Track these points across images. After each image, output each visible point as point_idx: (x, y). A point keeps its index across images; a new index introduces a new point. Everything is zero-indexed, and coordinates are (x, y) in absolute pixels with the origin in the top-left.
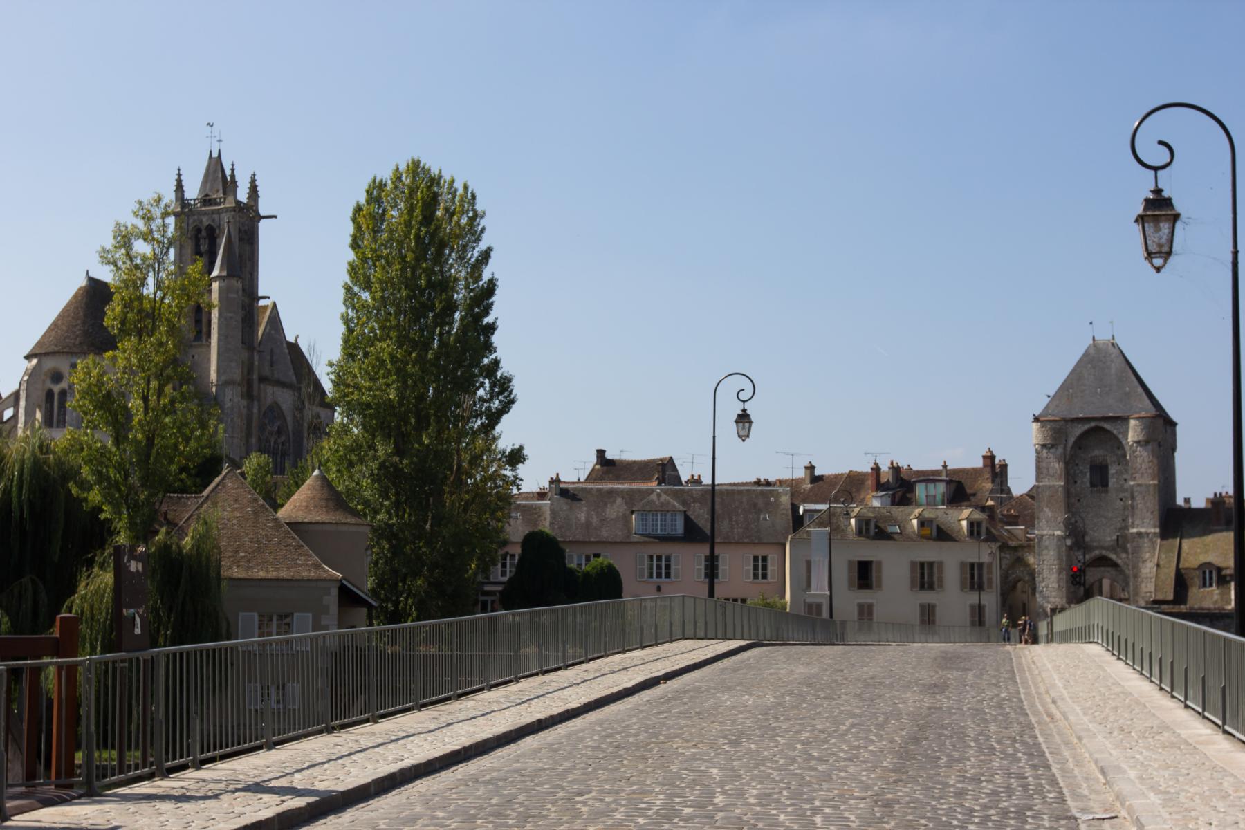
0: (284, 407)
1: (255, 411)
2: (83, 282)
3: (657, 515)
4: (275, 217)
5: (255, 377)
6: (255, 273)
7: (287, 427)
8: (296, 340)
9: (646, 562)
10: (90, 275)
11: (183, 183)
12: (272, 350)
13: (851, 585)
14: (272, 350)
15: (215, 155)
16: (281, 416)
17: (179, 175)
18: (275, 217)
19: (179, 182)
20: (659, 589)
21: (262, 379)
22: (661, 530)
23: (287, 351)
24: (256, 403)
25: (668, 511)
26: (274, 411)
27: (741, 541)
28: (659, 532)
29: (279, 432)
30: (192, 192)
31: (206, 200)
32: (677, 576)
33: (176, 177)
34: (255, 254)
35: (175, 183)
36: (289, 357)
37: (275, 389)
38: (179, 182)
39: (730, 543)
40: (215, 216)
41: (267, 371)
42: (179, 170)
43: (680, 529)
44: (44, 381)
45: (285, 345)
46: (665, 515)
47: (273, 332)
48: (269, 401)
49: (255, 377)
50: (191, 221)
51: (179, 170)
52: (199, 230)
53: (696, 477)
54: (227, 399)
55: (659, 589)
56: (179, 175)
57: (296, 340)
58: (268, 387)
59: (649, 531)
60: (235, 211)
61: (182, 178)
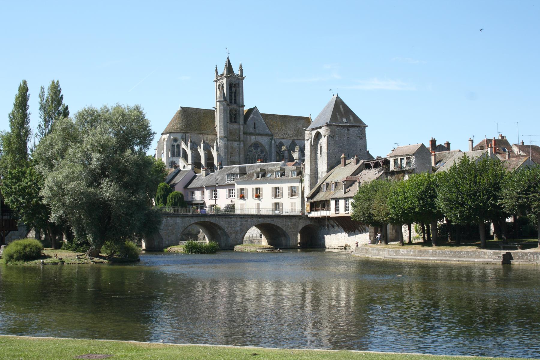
0: (263, 143)
1: (242, 145)
2: (179, 109)
5: (241, 133)
12: (255, 124)
13: (253, 197)
14: (255, 124)
16: (262, 146)
17: (216, 67)
19: (216, 70)
26: (256, 145)
29: (262, 151)
37: (256, 137)
38: (216, 70)
41: (251, 130)
47: (255, 117)
49: (241, 133)
56: (216, 67)
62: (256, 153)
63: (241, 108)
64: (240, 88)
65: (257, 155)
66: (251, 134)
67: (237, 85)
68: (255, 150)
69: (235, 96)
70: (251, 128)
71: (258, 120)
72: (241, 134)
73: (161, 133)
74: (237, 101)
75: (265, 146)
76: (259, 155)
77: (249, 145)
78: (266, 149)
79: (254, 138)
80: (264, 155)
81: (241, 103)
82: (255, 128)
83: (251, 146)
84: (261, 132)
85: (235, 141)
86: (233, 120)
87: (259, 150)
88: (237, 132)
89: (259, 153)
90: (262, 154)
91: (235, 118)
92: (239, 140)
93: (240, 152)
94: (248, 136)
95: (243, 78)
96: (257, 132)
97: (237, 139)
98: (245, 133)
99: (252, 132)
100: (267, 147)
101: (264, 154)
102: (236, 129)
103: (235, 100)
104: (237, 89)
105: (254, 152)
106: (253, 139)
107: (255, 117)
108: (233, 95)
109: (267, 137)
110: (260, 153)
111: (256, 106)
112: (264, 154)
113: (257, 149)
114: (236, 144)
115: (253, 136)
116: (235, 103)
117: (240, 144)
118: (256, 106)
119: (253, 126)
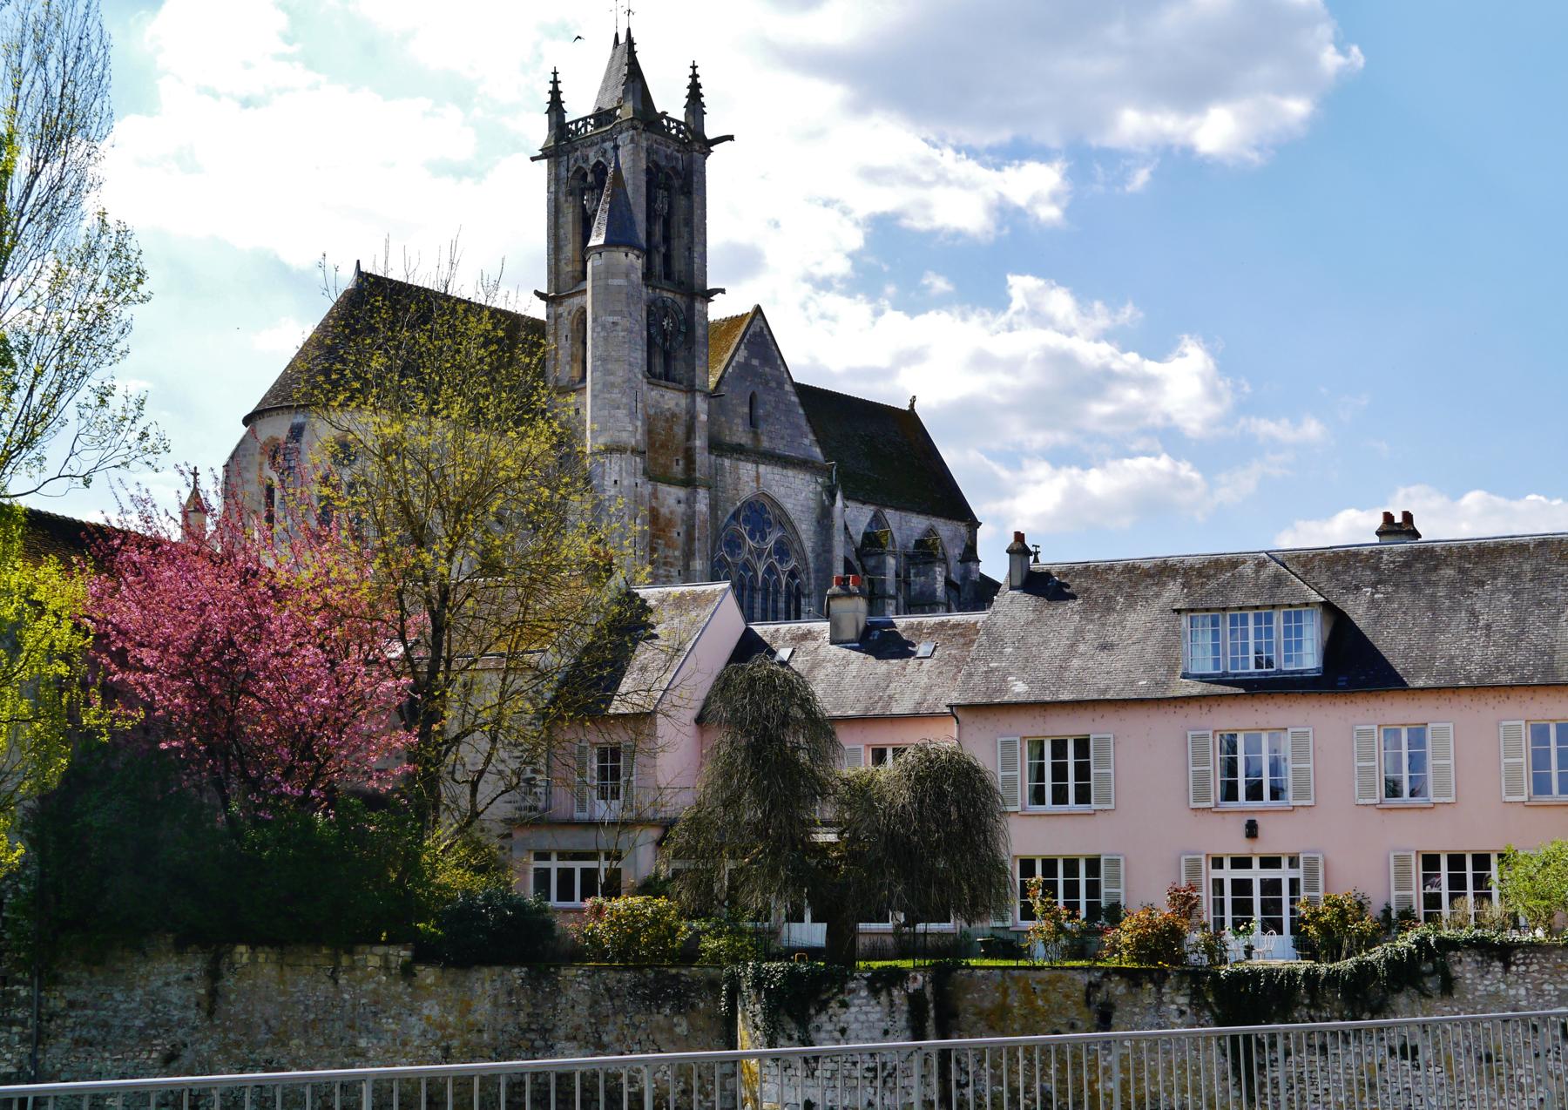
0: (788, 505)
1: (702, 506)
3: (1245, 621)
4: (731, 138)
5: (699, 442)
6: (697, 249)
7: (801, 543)
8: (912, 406)
9: (1215, 760)
10: (363, 269)
11: (563, 97)
15: (622, 39)
16: (784, 521)
18: (731, 138)
19: (555, 94)
20: (1252, 830)
21: (718, 446)
22: (1258, 665)
23: (795, 399)
24: (703, 496)
25: (1273, 607)
26: (760, 513)
27: (1487, 681)
28: (1252, 668)
29: (782, 550)
30: (579, 105)
31: (602, 117)
32: (1301, 793)
33: (550, 87)
34: (697, 212)
35: (548, 97)
36: (801, 411)
37: (762, 468)
38: (555, 94)
39: (1456, 689)
40: (609, 145)
41: (739, 434)
42: (555, 73)
43: (1310, 659)
44: (261, 464)
45: (788, 387)
46: (1269, 620)
47: (755, 362)
48: (747, 491)
49: (699, 442)
50: (572, 162)
51: (555, 73)
52: (581, 174)
53: (1398, 519)
54: (608, 482)
55: (1252, 830)
56: (555, 82)
57: (912, 406)
58: (742, 464)
59: (1226, 666)
60: (635, 128)
61: (560, 87)
62: (759, 557)
63: (698, 306)
64: (696, 199)
65: (761, 569)
66: (738, 451)
67: (677, 183)
68: (752, 538)
69: (667, 239)
70: (738, 421)
71: (767, 383)
72: (698, 443)
73: (249, 408)
74: (678, 265)
75: (796, 523)
76: (770, 570)
77: (732, 510)
78: (804, 537)
79: (753, 473)
80: (793, 574)
81: (698, 281)
82: (753, 422)
83: (735, 516)
84: (781, 448)
85: (670, 482)
86: (659, 368)
87: (771, 542)
88: (680, 431)
89: (769, 555)
90: (781, 561)
91: (668, 357)
92: (689, 482)
93: (690, 537)
94: (727, 462)
95: (707, 145)
96: (765, 444)
97: (678, 469)
98: (718, 446)
99: (743, 441)
100: (806, 530)
101: (793, 563)
102: (674, 415)
103: (667, 258)
104: (682, 202)
105: (750, 552)
106: (747, 478)
107: (755, 362)
108: (658, 230)
109: (808, 477)
110: (774, 559)
111: (758, 310)
112: (793, 563)
113: (763, 538)
114: (671, 497)
115: (750, 466)
116: (668, 275)
117: (690, 502)
118: (758, 310)
119: (746, 410)
